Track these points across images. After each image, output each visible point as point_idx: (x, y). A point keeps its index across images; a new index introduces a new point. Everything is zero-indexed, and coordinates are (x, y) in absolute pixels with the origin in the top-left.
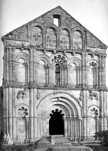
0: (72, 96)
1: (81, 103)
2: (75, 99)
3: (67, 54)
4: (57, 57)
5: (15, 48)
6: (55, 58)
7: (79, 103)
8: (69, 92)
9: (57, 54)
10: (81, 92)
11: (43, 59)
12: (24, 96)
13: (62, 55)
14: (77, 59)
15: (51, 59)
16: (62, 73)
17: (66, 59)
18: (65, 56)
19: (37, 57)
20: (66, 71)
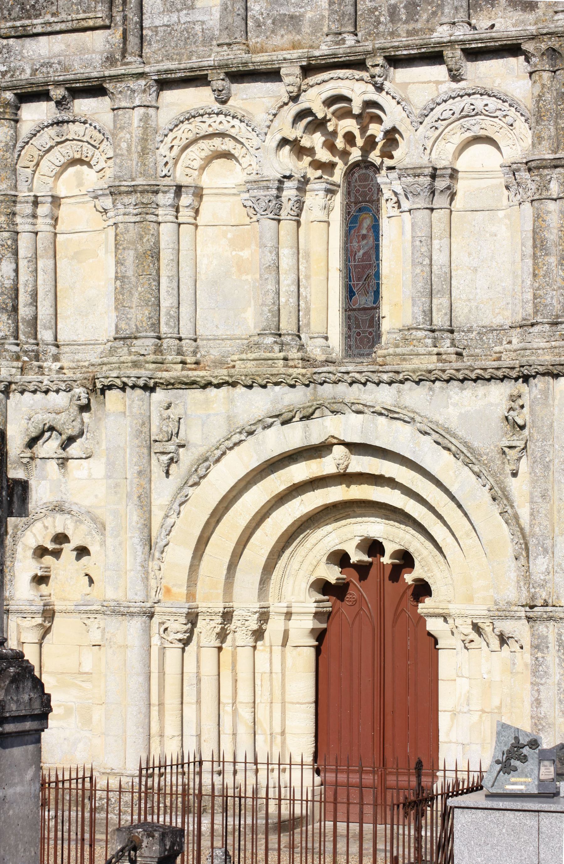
0: (443, 439)
1: (519, 488)
2: (467, 456)
3: (402, 75)
4: (320, 112)
5: (9, 96)
7: (501, 496)
8: (414, 397)
9: (312, 92)
10: (513, 398)
11: (207, 146)
12: (74, 449)
13: (360, 87)
14: (493, 103)
16: (397, 233)
17: (393, 116)
19: (168, 139)
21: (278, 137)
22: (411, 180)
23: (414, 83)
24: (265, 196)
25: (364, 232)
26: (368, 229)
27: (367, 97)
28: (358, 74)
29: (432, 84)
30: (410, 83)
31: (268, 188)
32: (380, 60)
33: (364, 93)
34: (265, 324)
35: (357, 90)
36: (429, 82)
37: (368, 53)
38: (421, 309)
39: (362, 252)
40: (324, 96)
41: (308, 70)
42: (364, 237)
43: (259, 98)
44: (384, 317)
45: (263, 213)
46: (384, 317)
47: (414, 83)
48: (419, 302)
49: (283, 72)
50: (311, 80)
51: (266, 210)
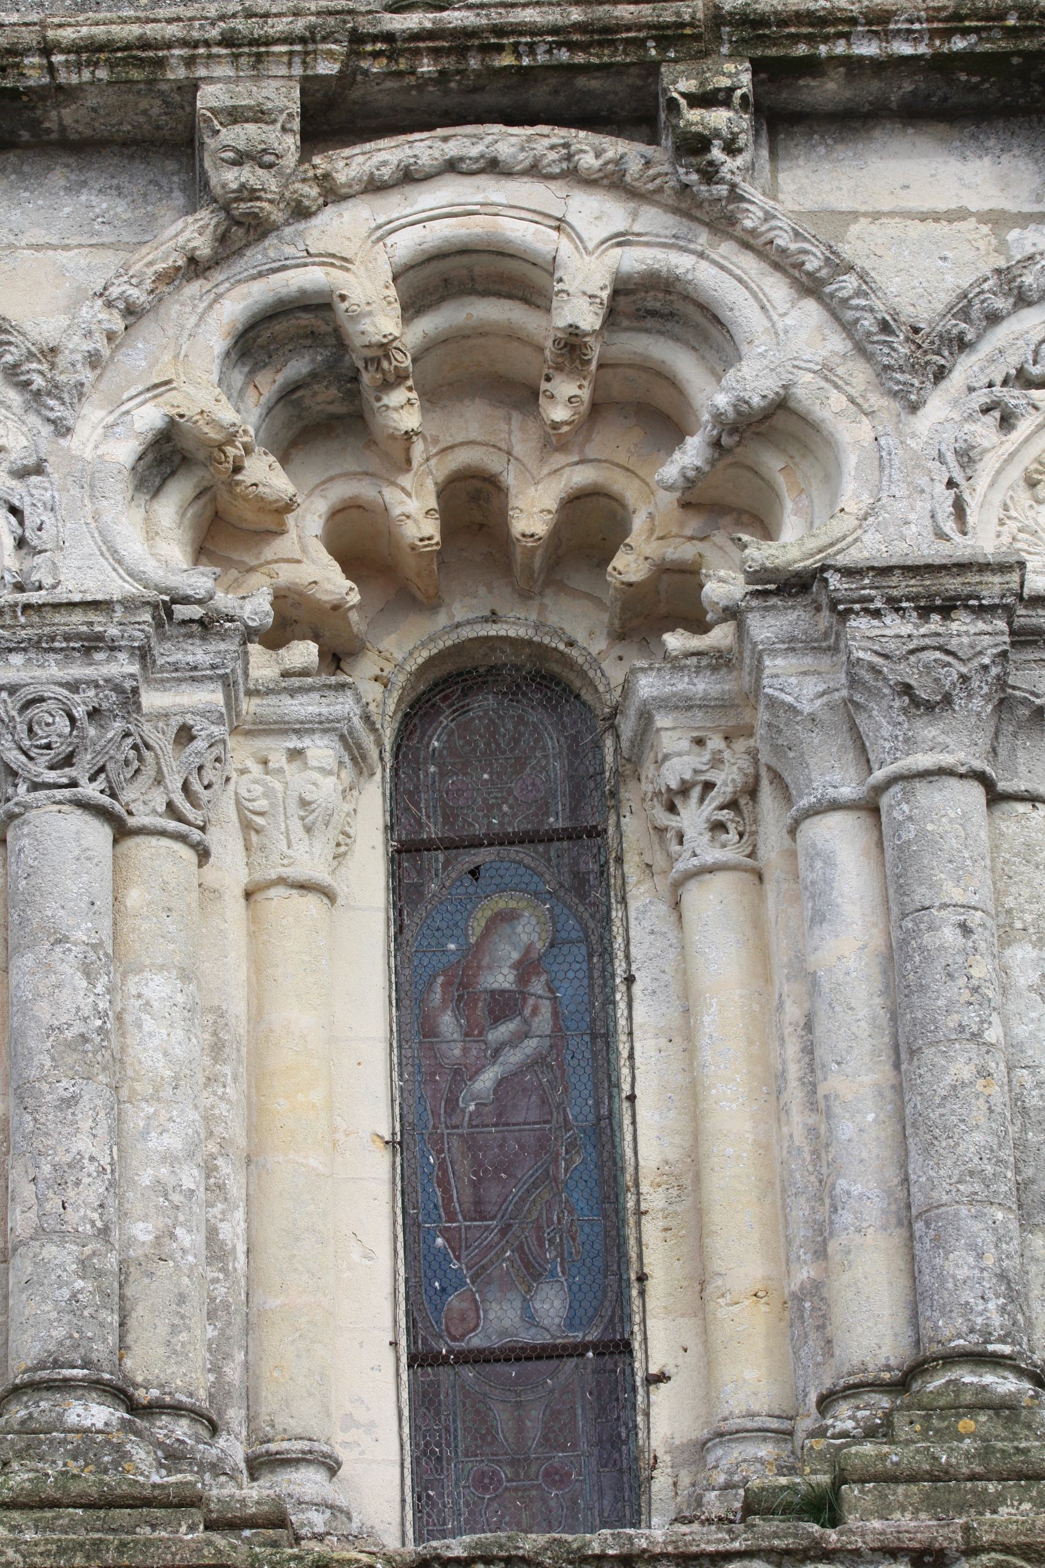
4: (376, 314)
6: (314, 375)
9: (341, 227)
13: (595, 214)
15: (109, 436)
17: (780, 343)
18: (715, 272)
20: (839, 838)
21: (149, 417)
22: (906, 629)
23: (876, 216)
24: (73, 687)
25: (503, 979)
26: (526, 968)
27: (635, 260)
28: (592, 148)
29: (972, 222)
30: (855, 215)
31: (91, 645)
32: (736, 74)
33: (621, 240)
34: (58, 1333)
35: (580, 227)
36: (959, 215)
37: (670, 36)
38: (989, 1260)
39: (486, 1080)
40: (406, 243)
41: (331, 118)
42: (504, 1007)
43: (37, 247)
44: (661, 1378)
45: (51, 776)
46: (661, 1378)
47: (876, 216)
48: (977, 1226)
49: (211, 96)
50: (352, 163)
51: (68, 761)
